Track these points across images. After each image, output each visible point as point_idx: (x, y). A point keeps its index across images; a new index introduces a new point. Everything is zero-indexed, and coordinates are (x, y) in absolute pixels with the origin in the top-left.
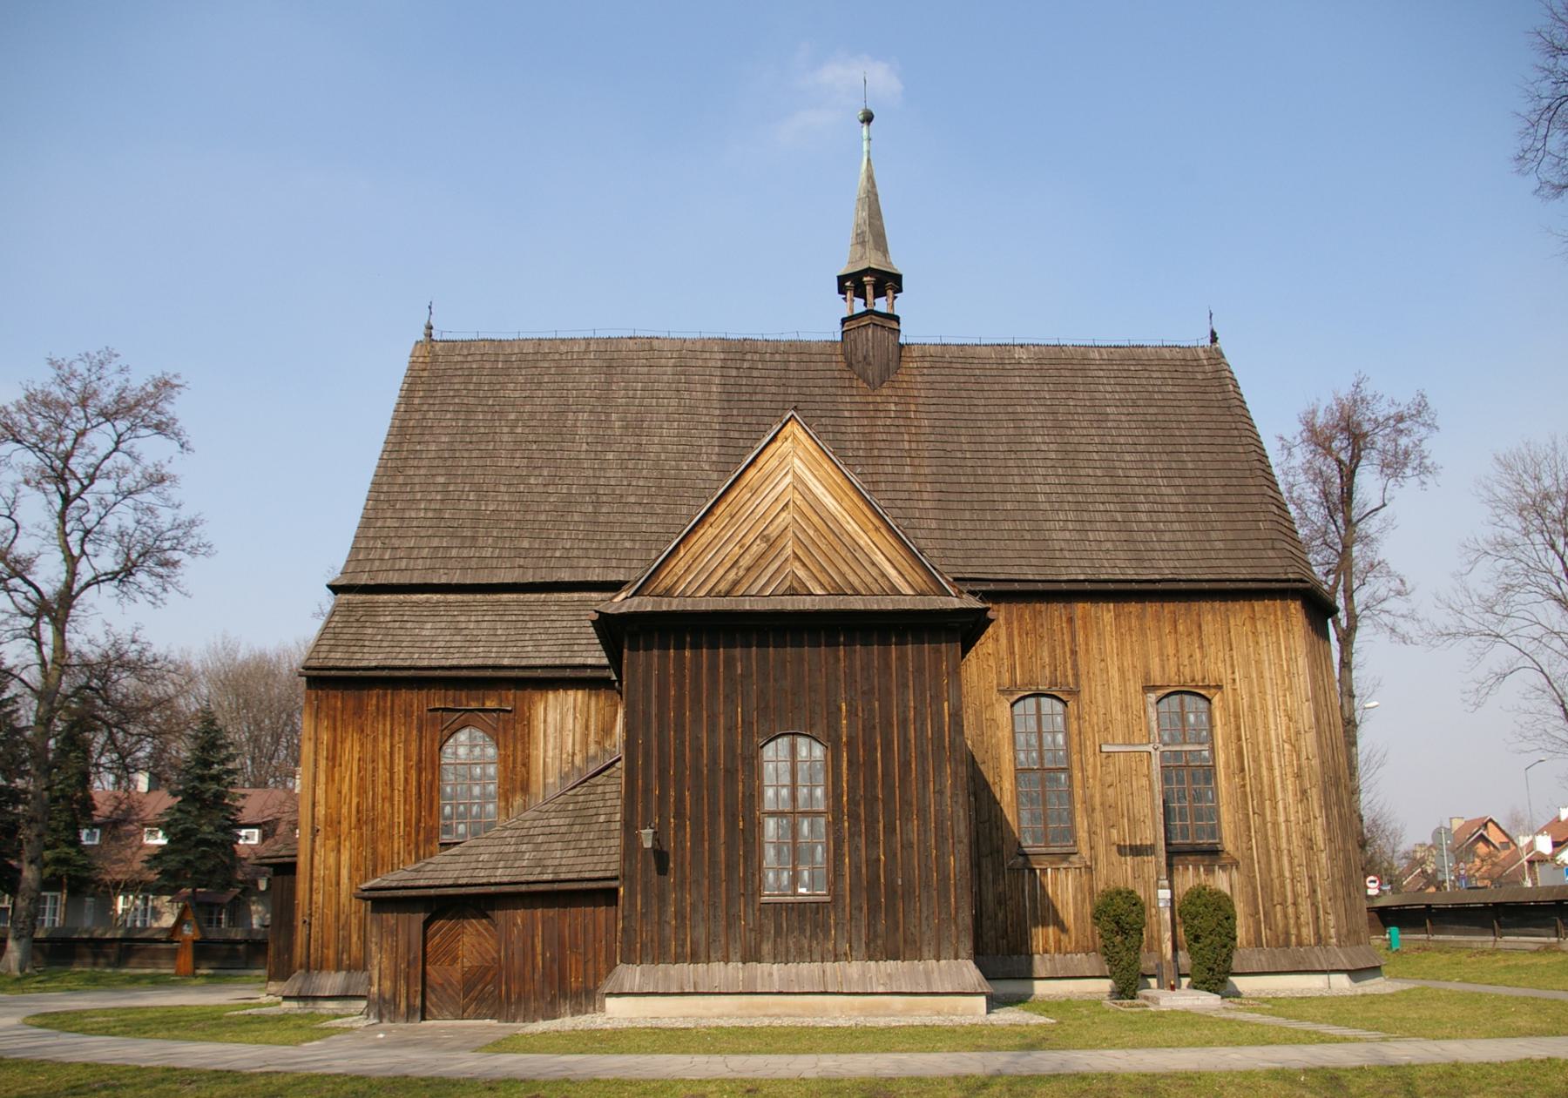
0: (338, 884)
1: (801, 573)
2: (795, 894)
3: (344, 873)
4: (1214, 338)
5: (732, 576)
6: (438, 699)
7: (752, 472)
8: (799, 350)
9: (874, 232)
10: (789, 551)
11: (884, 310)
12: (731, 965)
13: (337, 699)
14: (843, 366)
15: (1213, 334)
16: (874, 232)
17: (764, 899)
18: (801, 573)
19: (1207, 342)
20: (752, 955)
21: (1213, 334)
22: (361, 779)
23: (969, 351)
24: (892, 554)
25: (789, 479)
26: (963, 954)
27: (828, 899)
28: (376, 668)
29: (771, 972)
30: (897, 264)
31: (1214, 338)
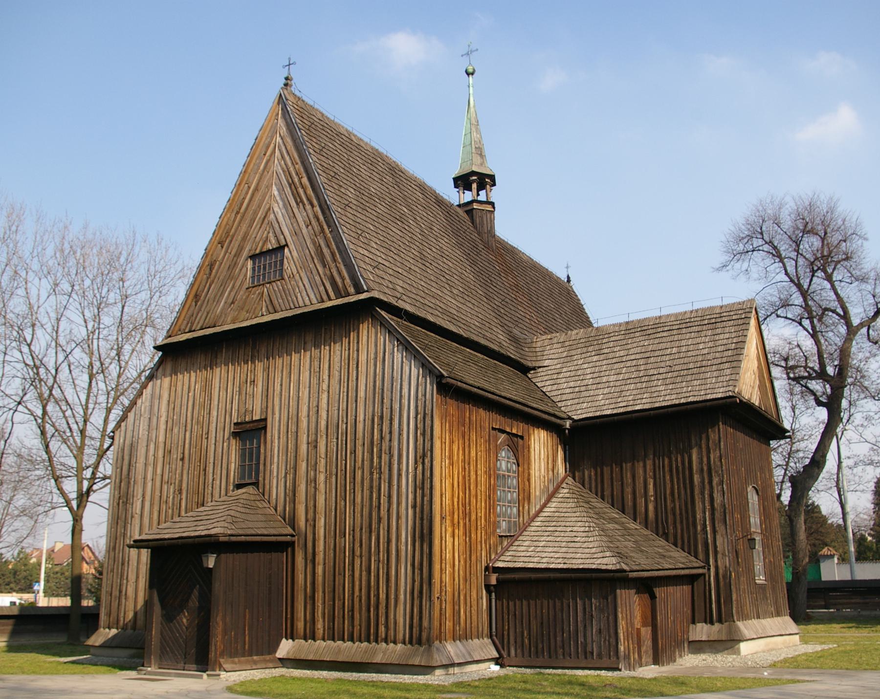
6: (498, 421)
13: (453, 406)
15: (568, 277)
21: (568, 277)
22: (464, 477)
27: (764, 582)
28: (479, 388)
31: (569, 280)
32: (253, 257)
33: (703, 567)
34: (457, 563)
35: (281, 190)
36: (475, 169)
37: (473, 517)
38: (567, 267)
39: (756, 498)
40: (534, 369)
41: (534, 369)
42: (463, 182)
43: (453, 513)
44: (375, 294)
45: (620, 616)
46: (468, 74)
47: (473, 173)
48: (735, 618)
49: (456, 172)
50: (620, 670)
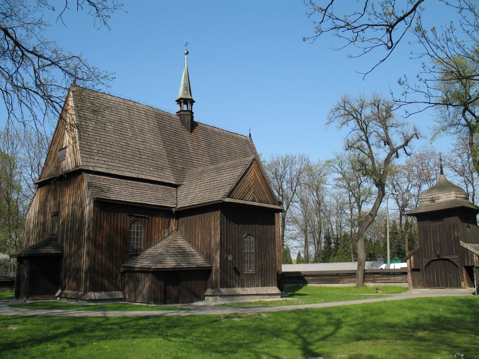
1: (255, 196)
5: (243, 195)
8: (169, 116)
9: (188, 88)
10: (253, 191)
11: (186, 109)
14: (181, 124)
15: (250, 134)
16: (188, 88)
19: (248, 136)
21: (250, 134)
23: (205, 126)
24: (269, 194)
26: (276, 285)
27: (255, 273)
30: (194, 99)
31: (250, 136)
32: (59, 150)
38: (250, 130)
40: (180, 185)
41: (180, 185)
42: (179, 101)
46: (185, 54)
47: (181, 99)
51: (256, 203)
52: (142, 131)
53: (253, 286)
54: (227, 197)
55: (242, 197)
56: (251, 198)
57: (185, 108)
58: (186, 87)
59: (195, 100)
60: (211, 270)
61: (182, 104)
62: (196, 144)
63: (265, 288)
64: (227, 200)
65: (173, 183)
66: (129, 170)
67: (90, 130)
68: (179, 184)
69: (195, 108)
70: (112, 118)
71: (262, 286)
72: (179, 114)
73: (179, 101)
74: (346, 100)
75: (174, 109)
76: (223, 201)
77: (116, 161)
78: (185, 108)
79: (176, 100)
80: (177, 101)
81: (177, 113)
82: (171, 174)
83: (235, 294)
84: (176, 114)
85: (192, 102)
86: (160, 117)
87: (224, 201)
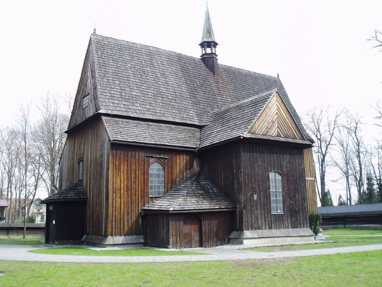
0: (121, 209)
1: (279, 131)
2: (277, 212)
3: (122, 205)
4: (278, 76)
5: (266, 131)
7: (270, 104)
8: (191, 60)
10: (277, 126)
11: (210, 52)
12: (267, 230)
15: (278, 74)
17: (272, 213)
18: (279, 131)
20: (270, 228)
21: (278, 74)
25: (276, 107)
28: (134, 142)
29: (275, 232)
30: (217, 41)
31: (278, 76)
33: (235, 208)
34: (122, 208)
35: (89, 73)
36: (205, 40)
37: (133, 191)
39: (279, 177)
40: (204, 126)
42: (203, 45)
43: (121, 189)
44: (100, 112)
45: (171, 227)
47: (204, 42)
48: (244, 229)
49: (200, 41)
50: (169, 248)
51: (281, 138)
52: (163, 74)
53: (282, 227)
54: (248, 133)
55: (265, 133)
56: (275, 133)
57: (209, 51)
58: (209, 30)
59: (218, 43)
60: (235, 211)
61: (206, 47)
62: (221, 85)
63: (296, 229)
64: (248, 136)
65: (197, 124)
66: (150, 113)
67: (110, 76)
68: (202, 124)
69: (218, 50)
70: (133, 63)
71: (292, 228)
72: (202, 57)
73: (203, 45)
74: (377, 30)
75: (197, 53)
76: (243, 137)
77: (136, 105)
78: (209, 51)
79: (199, 44)
80: (200, 45)
81: (201, 56)
82: (195, 115)
83: (261, 236)
84: (200, 58)
85: (215, 44)
86: (181, 60)
87: (245, 136)
